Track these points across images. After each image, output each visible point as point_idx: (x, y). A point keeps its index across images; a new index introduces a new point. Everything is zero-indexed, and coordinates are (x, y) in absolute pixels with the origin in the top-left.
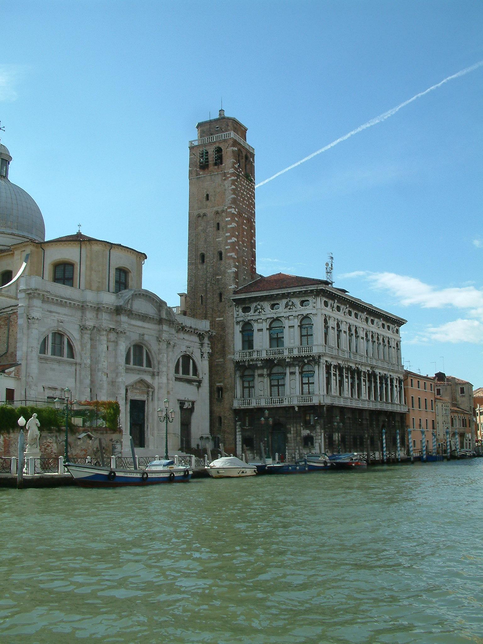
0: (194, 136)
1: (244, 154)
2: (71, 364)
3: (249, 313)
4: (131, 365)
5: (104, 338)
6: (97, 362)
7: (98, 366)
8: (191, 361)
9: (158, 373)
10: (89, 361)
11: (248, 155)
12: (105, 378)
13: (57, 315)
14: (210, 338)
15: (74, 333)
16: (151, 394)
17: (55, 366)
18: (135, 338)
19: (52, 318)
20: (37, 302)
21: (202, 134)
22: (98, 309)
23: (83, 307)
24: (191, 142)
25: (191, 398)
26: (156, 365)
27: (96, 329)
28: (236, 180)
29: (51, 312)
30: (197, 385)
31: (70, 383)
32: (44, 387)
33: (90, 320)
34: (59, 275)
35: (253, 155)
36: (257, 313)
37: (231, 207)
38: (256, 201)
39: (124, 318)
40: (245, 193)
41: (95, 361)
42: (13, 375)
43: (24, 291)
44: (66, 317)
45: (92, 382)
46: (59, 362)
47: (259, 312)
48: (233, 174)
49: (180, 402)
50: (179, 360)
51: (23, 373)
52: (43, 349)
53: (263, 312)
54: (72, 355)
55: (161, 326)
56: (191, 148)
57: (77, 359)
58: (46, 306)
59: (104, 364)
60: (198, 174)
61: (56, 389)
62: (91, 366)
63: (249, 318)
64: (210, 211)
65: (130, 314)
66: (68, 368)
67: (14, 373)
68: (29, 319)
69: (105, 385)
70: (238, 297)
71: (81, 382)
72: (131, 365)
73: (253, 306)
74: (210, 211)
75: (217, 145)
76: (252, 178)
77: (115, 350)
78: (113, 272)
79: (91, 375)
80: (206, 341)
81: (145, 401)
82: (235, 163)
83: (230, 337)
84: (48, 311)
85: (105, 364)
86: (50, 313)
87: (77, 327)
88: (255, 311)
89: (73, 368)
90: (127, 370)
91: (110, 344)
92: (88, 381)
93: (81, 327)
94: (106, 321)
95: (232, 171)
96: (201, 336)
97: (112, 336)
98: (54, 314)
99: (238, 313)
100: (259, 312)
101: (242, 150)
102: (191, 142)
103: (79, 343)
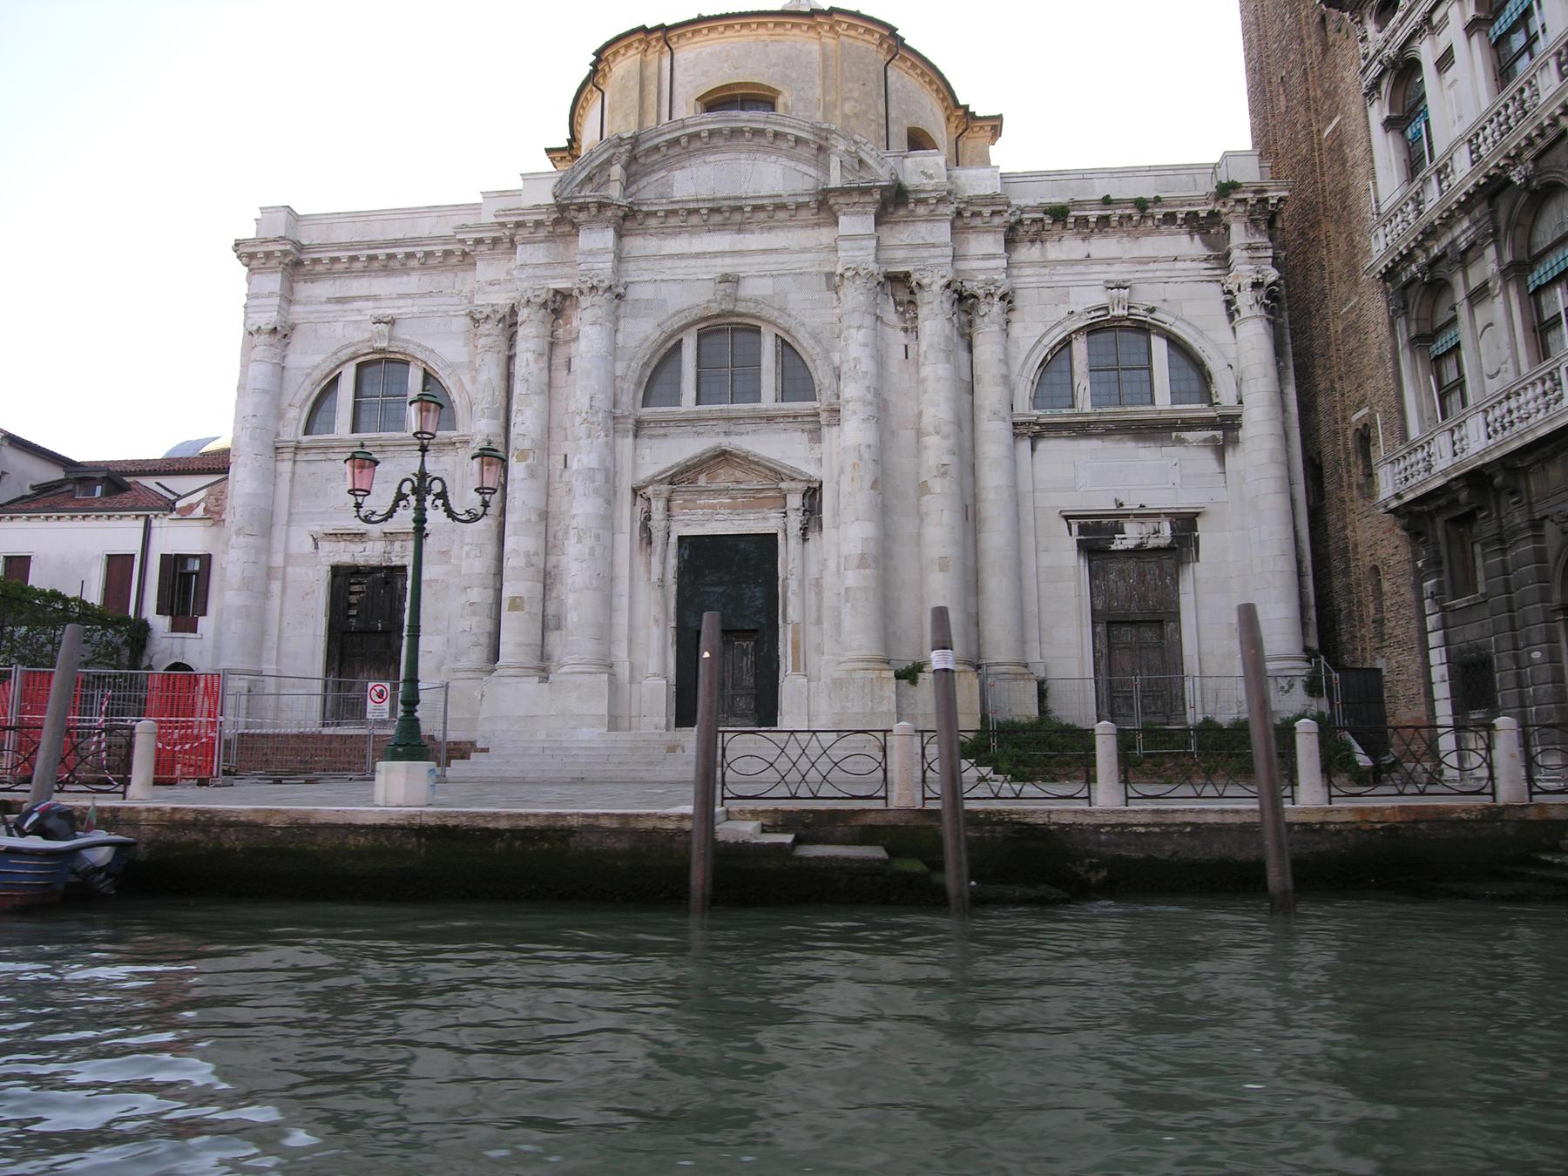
8: (1159, 346)
9: (835, 411)
13: (371, 304)
14: (1266, 217)
16: (795, 501)
19: (348, 319)
25: (1184, 501)
26: (826, 382)
29: (340, 300)
30: (1214, 438)
32: (315, 539)
42: (199, 512)
44: (409, 302)
49: (1081, 527)
50: (1066, 343)
67: (203, 505)
80: (1238, 235)
81: (776, 534)
84: (329, 301)
86: (339, 307)
96: (1205, 225)
98: (357, 305)
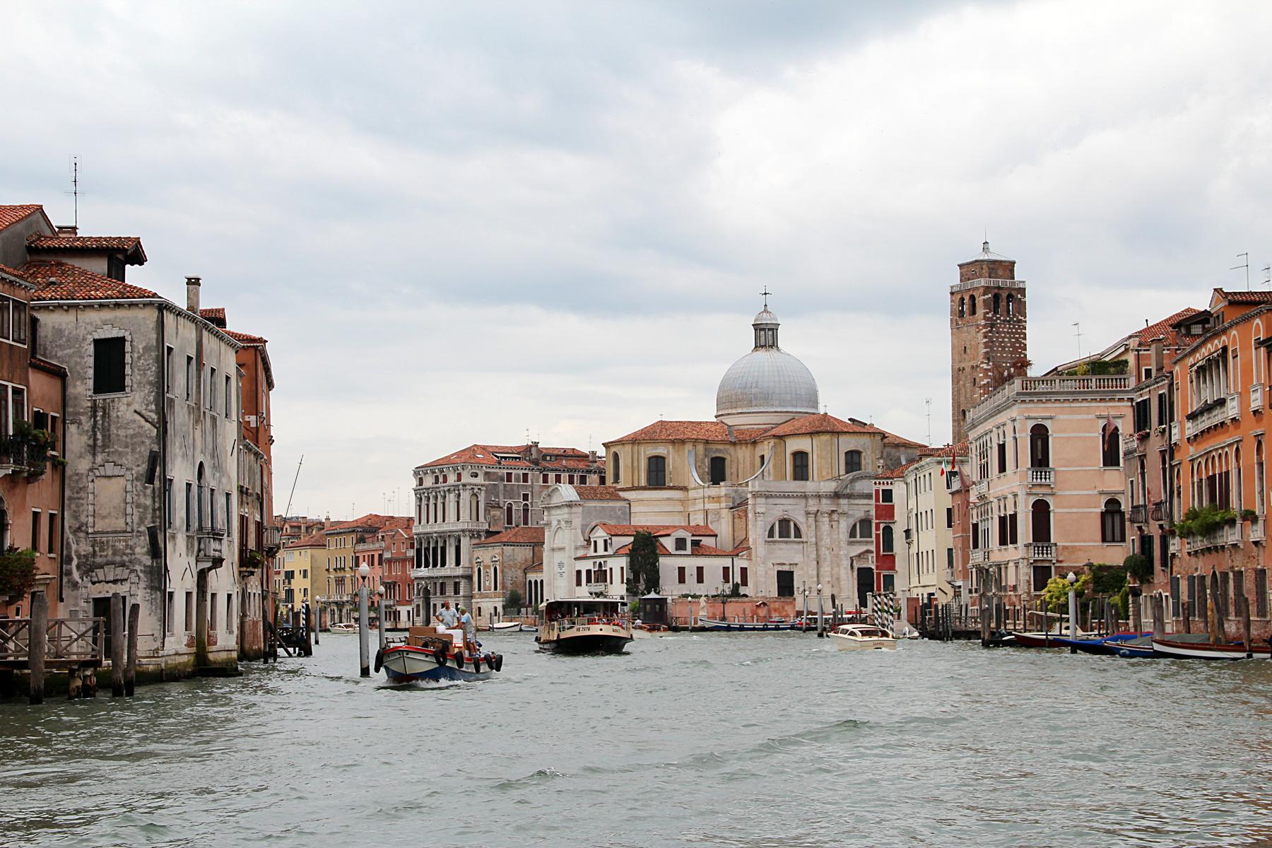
0: (956, 280)
1: (1004, 295)
2: (799, 542)
4: (858, 538)
5: (827, 519)
6: (821, 540)
10: (814, 539)
11: (1014, 293)
12: (827, 552)
15: (800, 518)
17: (783, 546)
18: (860, 514)
20: (761, 500)
21: (964, 278)
22: (819, 496)
23: (805, 496)
24: (952, 287)
28: (990, 331)
31: (798, 558)
33: (813, 505)
34: (798, 463)
35: (1022, 291)
37: (982, 363)
38: (1028, 342)
39: (843, 501)
40: (1006, 340)
42: (745, 557)
43: (751, 492)
45: (818, 555)
46: (786, 542)
48: (985, 326)
51: (753, 554)
52: (771, 534)
54: (798, 534)
56: (952, 294)
57: (804, 539)
58: (771, 501)
59: (826, 541)
60: (957, 324)
61: (784, 564)
62: (816, 544)
64: (967, 365)
65: (849, 496)
66: (796, 546)
69: (828, 558)
71: (808, 557)
72: (858, 538)
74: (967, 365)
75: (971, 293)
76: (1020, 318)
77: (838, 528)
78: (842, 457)
79: (817, 550)
82: (988, 313)
85: (828, 541)
87: (804, 512)
89: (801, 545)
90: (850, 543)
91: (833, 523)
92: (813, 556)
94: (826, 505)
95: (983, 322)
97: (835, 516)
101: (1001, 292)
102: (952, 287)
103: (805, 526)
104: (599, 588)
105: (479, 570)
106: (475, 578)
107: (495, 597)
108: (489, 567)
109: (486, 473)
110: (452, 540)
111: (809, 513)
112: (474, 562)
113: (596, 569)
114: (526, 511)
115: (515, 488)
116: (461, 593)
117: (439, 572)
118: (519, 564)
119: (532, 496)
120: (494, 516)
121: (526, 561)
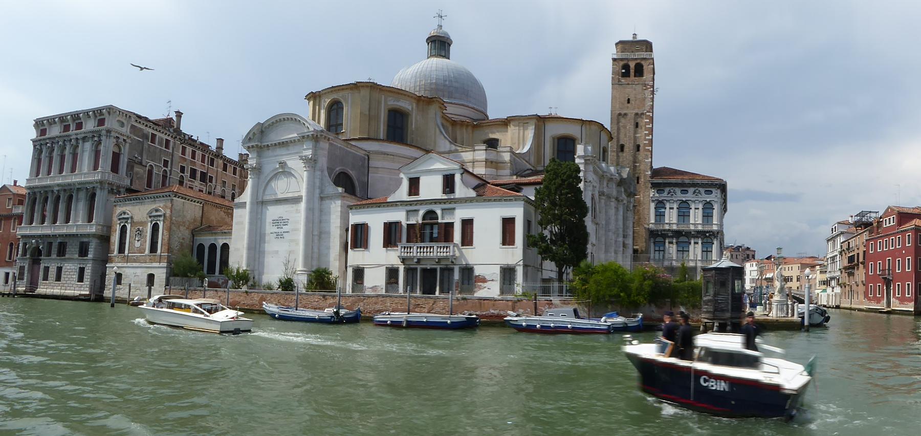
3: (663, 195)
7: (609, 227)
10: (604, 223)
27: (609, 197)
36: (669, 195)
41: (607, 224)
47: (672, 195)
53: (675, 196)
55: (629, 198)
63: (663, 198)
68: (587, 182)
70: (655, 181)
73: (667, 190)
83: (646, 213)
88: (669, 193)
93: (599, 193)
99: (652, 193)
100: (672, 195)
104: (435, 252)
105: (123, 230)
106: (115, 239)
107: (151, 261)
108: (143, 224)
109: (133, 126)
110: (82, 195)
111: (604, 195)
112: (115, 219)
113: (418, 219)
114: (165, 177)
115: (158, 151)
116: (90, 256)
117: (61, 229)
118: (188, 223)
119: (172, 164)
120: (137, 173)
121: (195, 220)
